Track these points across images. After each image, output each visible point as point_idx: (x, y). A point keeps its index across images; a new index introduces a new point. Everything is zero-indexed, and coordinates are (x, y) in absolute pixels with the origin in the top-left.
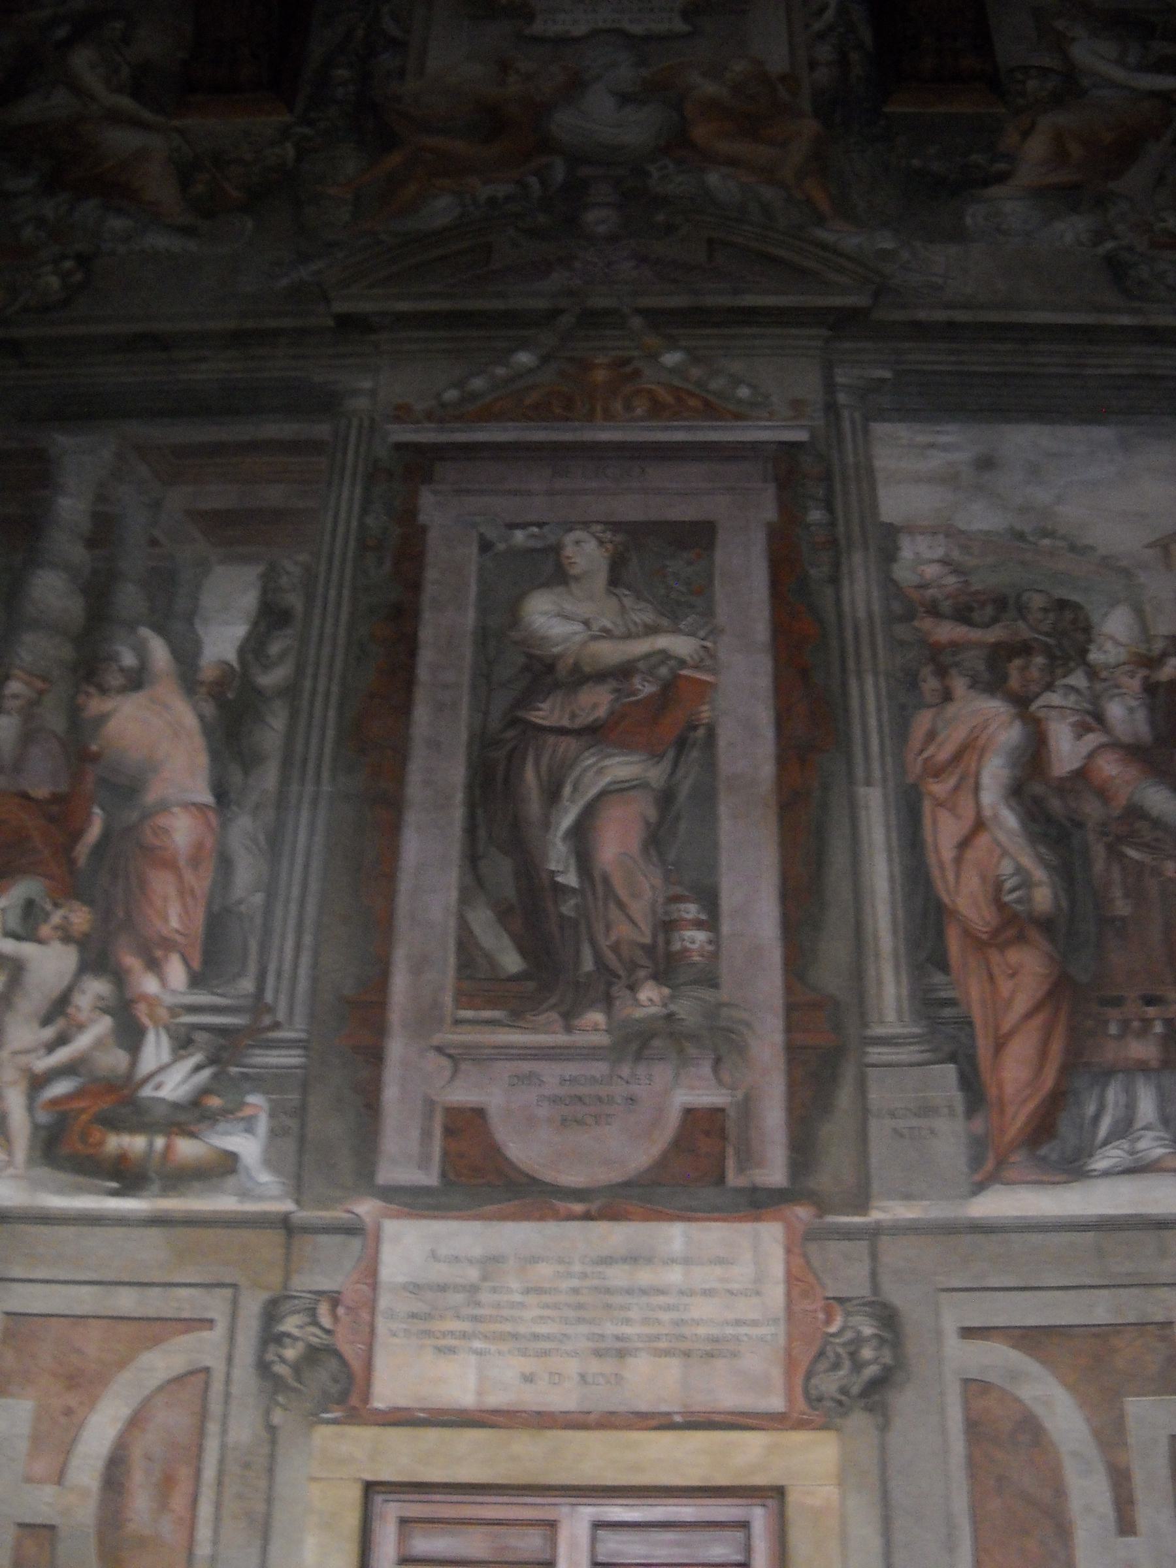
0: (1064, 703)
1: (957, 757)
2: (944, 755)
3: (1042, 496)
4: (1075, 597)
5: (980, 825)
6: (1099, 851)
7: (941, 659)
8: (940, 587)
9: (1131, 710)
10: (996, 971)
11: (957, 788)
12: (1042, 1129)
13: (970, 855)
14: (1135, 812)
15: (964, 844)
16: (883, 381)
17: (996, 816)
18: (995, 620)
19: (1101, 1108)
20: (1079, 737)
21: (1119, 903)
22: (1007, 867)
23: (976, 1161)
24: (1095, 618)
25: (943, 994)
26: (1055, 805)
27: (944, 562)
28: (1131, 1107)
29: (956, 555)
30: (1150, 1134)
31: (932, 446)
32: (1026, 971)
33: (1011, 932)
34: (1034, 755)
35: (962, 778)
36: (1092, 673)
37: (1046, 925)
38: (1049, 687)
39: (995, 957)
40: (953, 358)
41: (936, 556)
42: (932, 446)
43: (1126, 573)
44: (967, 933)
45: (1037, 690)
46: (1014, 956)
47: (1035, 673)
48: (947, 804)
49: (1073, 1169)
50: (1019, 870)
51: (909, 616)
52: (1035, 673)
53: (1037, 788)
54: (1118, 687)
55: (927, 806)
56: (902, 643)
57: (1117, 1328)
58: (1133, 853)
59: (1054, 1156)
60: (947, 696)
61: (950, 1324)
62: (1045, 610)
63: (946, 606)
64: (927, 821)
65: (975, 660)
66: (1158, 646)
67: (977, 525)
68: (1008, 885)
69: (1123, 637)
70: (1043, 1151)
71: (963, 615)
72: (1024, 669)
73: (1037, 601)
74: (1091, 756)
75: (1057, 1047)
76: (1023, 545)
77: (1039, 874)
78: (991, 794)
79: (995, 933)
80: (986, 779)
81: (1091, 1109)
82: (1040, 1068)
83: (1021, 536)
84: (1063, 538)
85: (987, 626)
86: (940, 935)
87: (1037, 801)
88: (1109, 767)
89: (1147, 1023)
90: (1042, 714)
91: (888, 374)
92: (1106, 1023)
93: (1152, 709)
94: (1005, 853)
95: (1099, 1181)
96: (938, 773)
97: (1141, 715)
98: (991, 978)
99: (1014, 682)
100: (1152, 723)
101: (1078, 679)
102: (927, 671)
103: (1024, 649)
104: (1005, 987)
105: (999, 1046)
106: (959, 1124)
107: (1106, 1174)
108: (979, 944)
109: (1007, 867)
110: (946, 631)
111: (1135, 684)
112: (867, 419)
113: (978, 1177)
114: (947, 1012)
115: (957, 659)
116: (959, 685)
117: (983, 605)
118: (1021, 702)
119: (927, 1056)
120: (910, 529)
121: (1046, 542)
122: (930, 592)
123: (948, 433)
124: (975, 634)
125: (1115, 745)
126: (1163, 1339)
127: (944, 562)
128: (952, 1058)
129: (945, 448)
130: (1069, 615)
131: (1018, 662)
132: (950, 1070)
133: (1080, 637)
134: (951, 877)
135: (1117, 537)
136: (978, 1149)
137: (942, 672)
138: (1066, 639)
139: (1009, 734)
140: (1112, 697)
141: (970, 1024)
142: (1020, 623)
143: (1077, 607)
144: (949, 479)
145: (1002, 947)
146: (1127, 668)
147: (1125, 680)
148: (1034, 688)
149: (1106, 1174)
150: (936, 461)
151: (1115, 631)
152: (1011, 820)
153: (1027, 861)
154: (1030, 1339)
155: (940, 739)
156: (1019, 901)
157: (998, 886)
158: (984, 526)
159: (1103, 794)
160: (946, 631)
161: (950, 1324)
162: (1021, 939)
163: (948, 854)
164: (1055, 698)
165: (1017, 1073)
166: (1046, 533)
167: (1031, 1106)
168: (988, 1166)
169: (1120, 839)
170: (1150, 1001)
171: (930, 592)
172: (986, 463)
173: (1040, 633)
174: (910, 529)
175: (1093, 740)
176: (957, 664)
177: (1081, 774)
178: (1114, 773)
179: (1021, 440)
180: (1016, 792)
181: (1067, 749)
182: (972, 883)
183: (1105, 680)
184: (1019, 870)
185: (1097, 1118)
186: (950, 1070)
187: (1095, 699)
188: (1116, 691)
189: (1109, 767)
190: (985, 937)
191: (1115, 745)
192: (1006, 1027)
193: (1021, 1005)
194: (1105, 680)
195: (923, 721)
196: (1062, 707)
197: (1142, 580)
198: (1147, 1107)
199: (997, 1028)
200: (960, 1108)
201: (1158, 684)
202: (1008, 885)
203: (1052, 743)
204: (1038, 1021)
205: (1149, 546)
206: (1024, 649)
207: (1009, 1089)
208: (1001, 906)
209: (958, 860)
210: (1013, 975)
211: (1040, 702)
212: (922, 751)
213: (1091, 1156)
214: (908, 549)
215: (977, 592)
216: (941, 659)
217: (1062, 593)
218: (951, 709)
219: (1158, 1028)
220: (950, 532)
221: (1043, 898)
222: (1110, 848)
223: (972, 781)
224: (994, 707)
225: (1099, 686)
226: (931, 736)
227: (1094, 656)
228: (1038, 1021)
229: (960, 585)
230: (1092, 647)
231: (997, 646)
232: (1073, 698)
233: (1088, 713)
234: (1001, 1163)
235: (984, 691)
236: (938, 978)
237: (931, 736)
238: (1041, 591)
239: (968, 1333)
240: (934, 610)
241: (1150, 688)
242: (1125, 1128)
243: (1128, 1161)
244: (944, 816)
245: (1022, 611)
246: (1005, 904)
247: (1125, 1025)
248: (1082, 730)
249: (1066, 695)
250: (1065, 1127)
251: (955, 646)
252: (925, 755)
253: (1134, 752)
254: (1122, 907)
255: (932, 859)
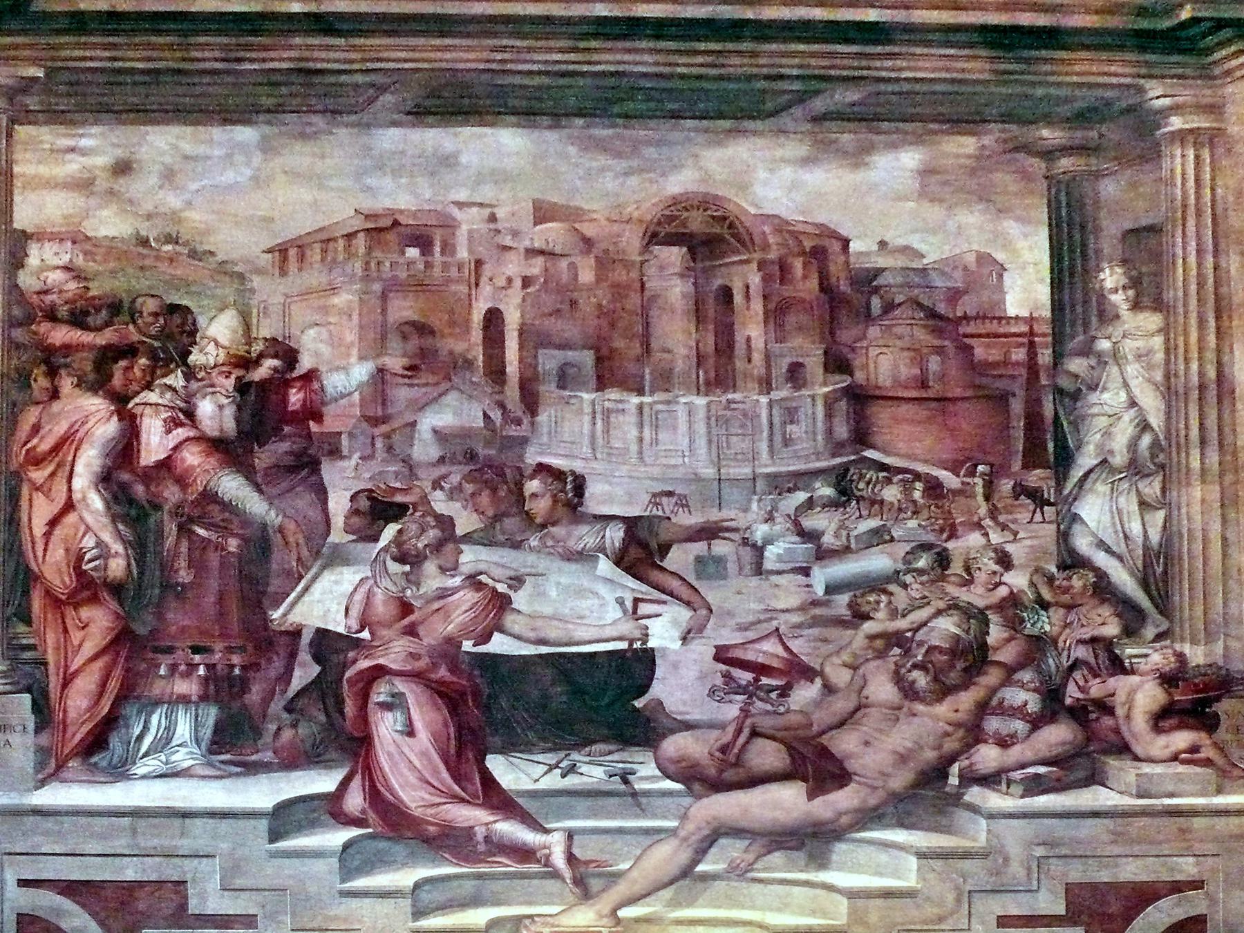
0: (160, 401)
1: (56, 448)
2: (45, 446)
3: (173, 201)
4: (184, 302)
5: (69, 506)
6: (171, 528)
7: (52, 360)
8: (61, 292)
9: (221, 407)
10: (69, 622)
11: (53, 474)
12: (96, 742)
13: (58, 532)
14: (209, 497)
15: (53, 523)
16: (35, 79)
17: (84, 499)
18: (108, 324)
19: (146, 728)
20: (169, 431)
21: (182, 573)
22: (89, 542)
23: (40, 766)
24: (202, 321)
25: (24, 642)
26: (139, 489)
27: (67, 268)
28: (170, 730)
29: (80, 261)
30: (183, 750)
31: (72, 150)
32: (98, 622)
33: (86, 594)
34: (126, 447)
35: (59, 466)
36: (190, 375)
37: (117, 589)
38: (148, 386)
39: (70, 612)
40: (107, 54)
41: (61, 263)
42: (72, 150)
43: (241, 277)
44: (48, 593)
45: (137, 389)
46: (85, 613)
47: (137, 372)
48: (43, 488)
49: (119, 772)
50: (100, 544)
51: (29, 320)
52: (137, 372)
53: (125, 476)
54: (212, 386)
55: (25, 491)
56: (18, 346)
57: (141, 884)
58: (201, 532)
59: (104, 763)
60: (55, 394)
61: (10, 877)
62: (156, 315)
63: (63, 312)
64: (24, 504)
65: (85, 362)
66: (258, 348)
67: (104, 231)
68: (87, 557)
69: (224, 341)
70: (94, 759)
71: (78, 319)
72: (128, 369)
73: (151, 305)
74: (176, 448)
75: (113, 685)
76: (145, 251)
77: (117, 547)
78: (82, 481)
79: (72, 595)
80: (79, 468)
81: (137, 731)
82: (97, 702)
83: (145, 242)
84: (186, 244)
85: (98, 329)
86: (26, 593)
87: (124, 487)
88: (192, 457)
89: (193, 667)
90: (138, 410)
91: (40, 74)
92: (158, 666)
93: (239, 408)
94: (88, 529)
95: (138, 782)
96: (37, 461)
97: (229, 412)
98: (66, 631)
99: (117, 381)
100: (238, 420)
101: (176, 379)
102: (39, 372)
103: (130, 351)
104: (76, 636)
105: (66, 683)
106: (30, 738)
107: (144, 777)
108: (56, 603)
109: (89, 542)
110: (61, 335)
111: (230, 383)
112: (13, 121)
113: (40, 776)
114: (28, 655)
115: (68, 360)
116: (67, 384)
117: (98, 310)
118: (120, 401)
119: (8, 688)
120: (40, 236)
121: (169, 247)
122: (49, 298)
123: (91, 135)
124: (87, 337)
125: (202, 439)
126: (176, 893)
127: (67, 268)
128: (28, 690)
129: (84, 152)
130: (177, 319)
131: (123, 363)
132: (27, 698)
133: (185, 340)
134: (40, 554)
135: (239, 242)
136: (43, 753)
137: (52, 373)
138: (176, 333)
139: (107, 429)
140: (204, 397)
141: (46, 664)
142: (131, 327)
143: (187, 310)
144: (84, 185)
145: (76, 606)
146: (224, 369)
147: (221, 380)
148: (135, 387)
149: (144, 777)
150: (73, 166)
151: (219, 331)
152: (97, 502)
153: (107, 537)
154: (69, 888)
155: (42, 432)
156: (95, 569)
157: (80, 558)
158: (111, 232)
159: (182, 481)
160: (61, 335)
161: (10, 877)
162: (94, 600)
163: (39, 529)
164: (153, 397)
165: (79, 702)
166: (169, 239)
167: (85, 729)
168: (51, 767)
169: (191, 520)
170: (196, 650)
171: (49, 298)
172: (123, 168)
173: (150, 337)
174: (40, 236)
175: (181, 433)
176: (66, 366)
177: (166, 465)
178: (196, 463)
179: (161, 142)
180: (105, 479)
181: (155, 441)
182: (57, 554)
183: (202, 380)
184: (100, 544)
185: (140, 738)
186: (27, 698)
187: (189, 399)
188: (210, 390)
189: (192, 457)
190: (64, 597)
191: (202, 439)
192: (73, 668)
193: (89, 649)
194: (202, 380)
195: (31, 416)
196: (157, 405)
197: (255, 284)
198: (184, 729)
199: (66, 667)
200: (31, 726)
201: (250, 384)
202: (87, 557)
203: (144, 437)
204: (99, 664)
205: (269, 251)
206: (130, 351)
207: (72, 714)
208: (80, 573)
209: (48, 535)
210: (83, 628)
211: (137, 400)
212: (25, 444)
213: (134, 763)
214: (36, 255)
215: (94, 298)
216: (52, 360)
217: (176, 299)
218: (56, 407)
219: (202, 671)
220: (78, 239)
221: (117, 567)
222: (180, 528)
223: (68, 468)
224: (96, 404)
225: (194, 385)
226: (36, 429)
227: (195, 358)
228: (99, 664)
229: (78, 291)
230: (195, 350)
231: (108, 348)
232: (168, 395)
233: (181, 410)
234: (60, 767)
235: (89, 389)
236: (22, 628)
237: (36, 429)
238: (153, 296)
239: (23, 883)
240: (51, 316)
241: (242, 388)
242: (164, 742)
243: (164, 769)
244: (39, 499)
245: (134, 315)
246: (85, 571)
247: (173, 668)
248: (172, 424)
249: (162, 394)
250: (115, 741)
251: (67, 349)
252: (29, 445)
253: (217, 446)
254: (184, 575)
255: (26, 536)
